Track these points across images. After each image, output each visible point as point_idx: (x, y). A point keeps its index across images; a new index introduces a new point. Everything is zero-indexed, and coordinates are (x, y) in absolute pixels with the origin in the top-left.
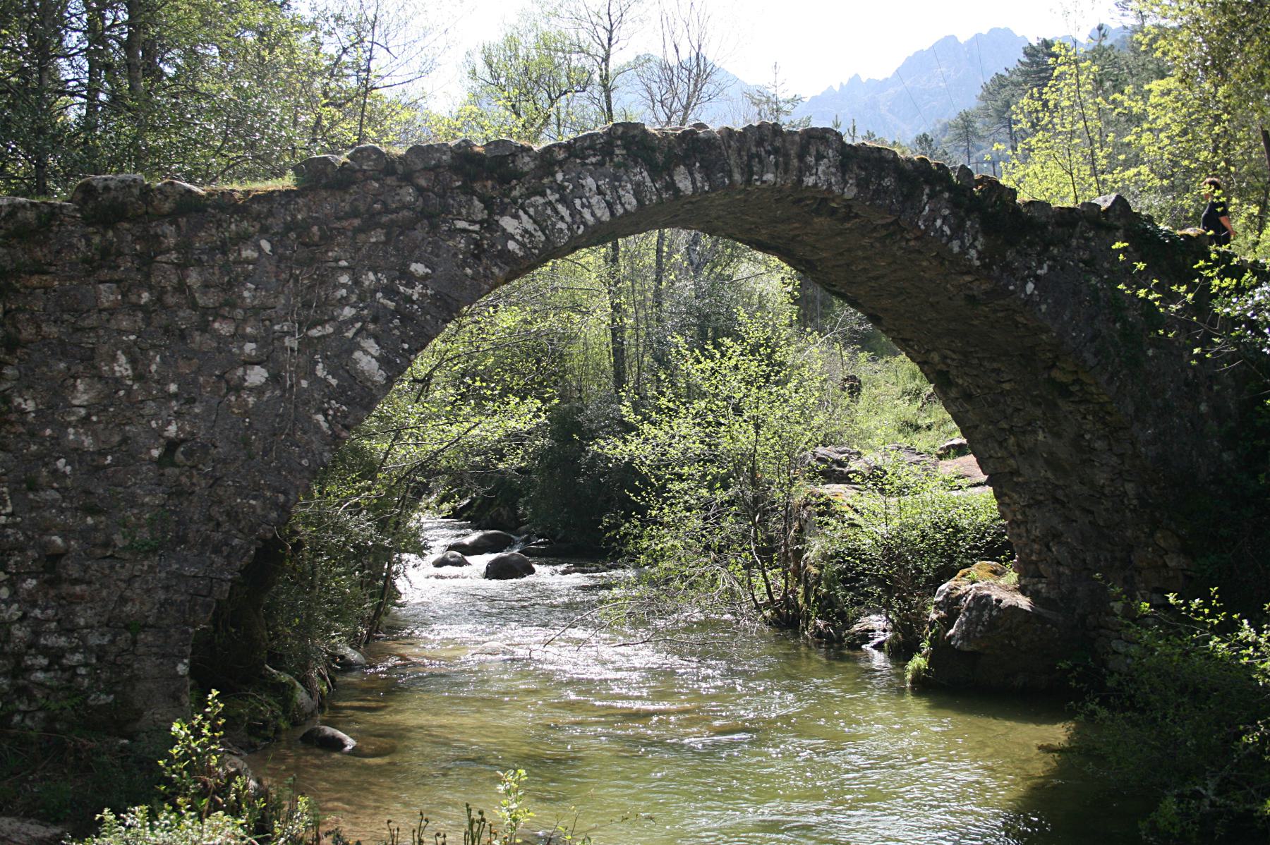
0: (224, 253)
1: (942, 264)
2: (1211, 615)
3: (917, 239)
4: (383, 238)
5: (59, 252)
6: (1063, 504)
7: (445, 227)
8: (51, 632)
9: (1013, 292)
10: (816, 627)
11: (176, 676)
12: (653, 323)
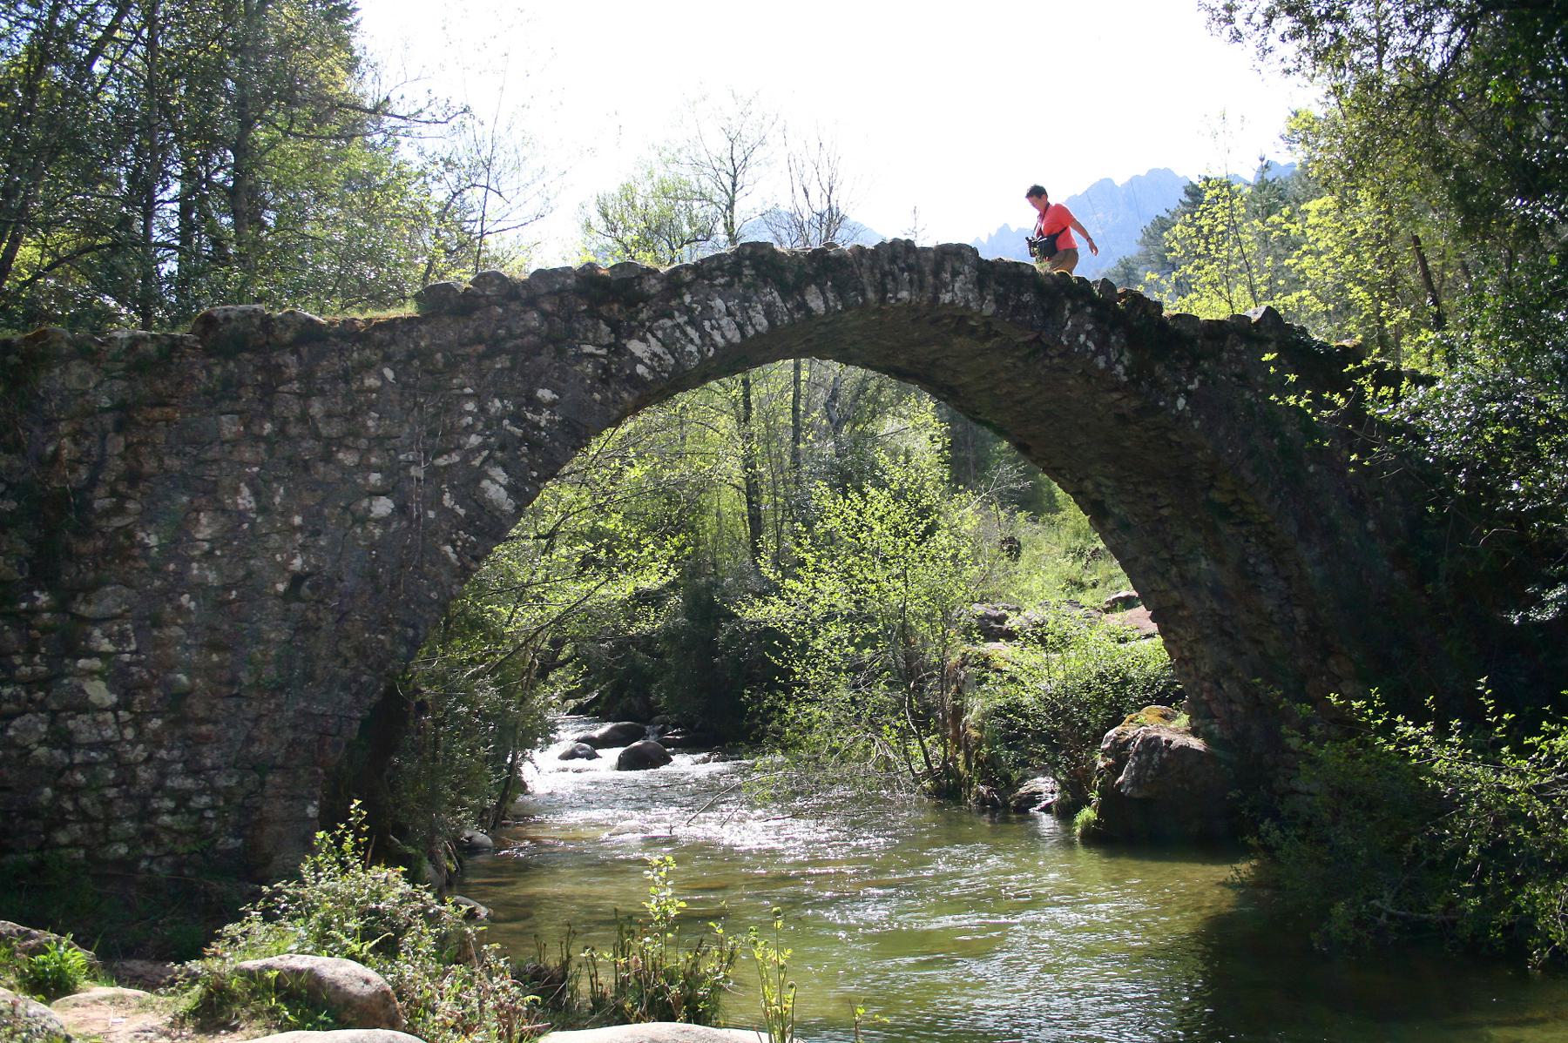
0: (347, 382)
1: (1088, 382)
2: (1375, 717)
3: (1060, 355)
4: (508, 364)
5: (180, 384)
6: (1230, 636)
7: (571, 352)
8: (177, 774)
9: (1163, 408)
10: (979, 793)
11: (306, 819)
12: (791, 486)
